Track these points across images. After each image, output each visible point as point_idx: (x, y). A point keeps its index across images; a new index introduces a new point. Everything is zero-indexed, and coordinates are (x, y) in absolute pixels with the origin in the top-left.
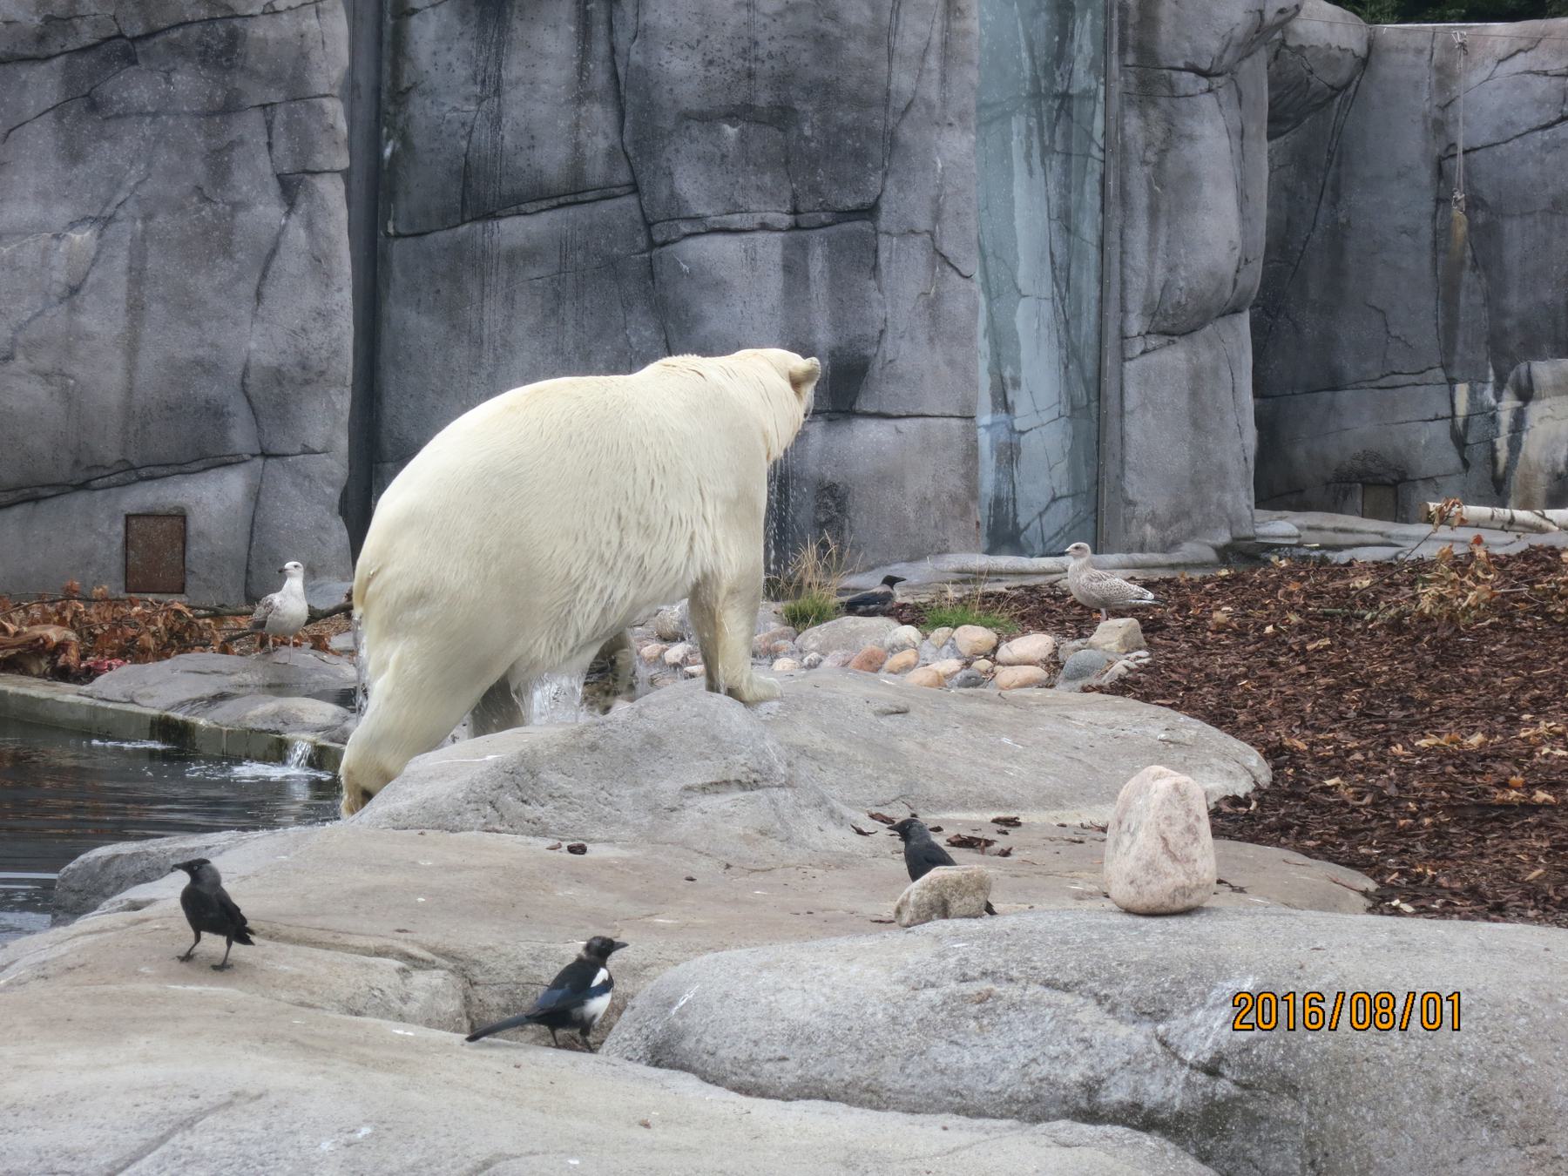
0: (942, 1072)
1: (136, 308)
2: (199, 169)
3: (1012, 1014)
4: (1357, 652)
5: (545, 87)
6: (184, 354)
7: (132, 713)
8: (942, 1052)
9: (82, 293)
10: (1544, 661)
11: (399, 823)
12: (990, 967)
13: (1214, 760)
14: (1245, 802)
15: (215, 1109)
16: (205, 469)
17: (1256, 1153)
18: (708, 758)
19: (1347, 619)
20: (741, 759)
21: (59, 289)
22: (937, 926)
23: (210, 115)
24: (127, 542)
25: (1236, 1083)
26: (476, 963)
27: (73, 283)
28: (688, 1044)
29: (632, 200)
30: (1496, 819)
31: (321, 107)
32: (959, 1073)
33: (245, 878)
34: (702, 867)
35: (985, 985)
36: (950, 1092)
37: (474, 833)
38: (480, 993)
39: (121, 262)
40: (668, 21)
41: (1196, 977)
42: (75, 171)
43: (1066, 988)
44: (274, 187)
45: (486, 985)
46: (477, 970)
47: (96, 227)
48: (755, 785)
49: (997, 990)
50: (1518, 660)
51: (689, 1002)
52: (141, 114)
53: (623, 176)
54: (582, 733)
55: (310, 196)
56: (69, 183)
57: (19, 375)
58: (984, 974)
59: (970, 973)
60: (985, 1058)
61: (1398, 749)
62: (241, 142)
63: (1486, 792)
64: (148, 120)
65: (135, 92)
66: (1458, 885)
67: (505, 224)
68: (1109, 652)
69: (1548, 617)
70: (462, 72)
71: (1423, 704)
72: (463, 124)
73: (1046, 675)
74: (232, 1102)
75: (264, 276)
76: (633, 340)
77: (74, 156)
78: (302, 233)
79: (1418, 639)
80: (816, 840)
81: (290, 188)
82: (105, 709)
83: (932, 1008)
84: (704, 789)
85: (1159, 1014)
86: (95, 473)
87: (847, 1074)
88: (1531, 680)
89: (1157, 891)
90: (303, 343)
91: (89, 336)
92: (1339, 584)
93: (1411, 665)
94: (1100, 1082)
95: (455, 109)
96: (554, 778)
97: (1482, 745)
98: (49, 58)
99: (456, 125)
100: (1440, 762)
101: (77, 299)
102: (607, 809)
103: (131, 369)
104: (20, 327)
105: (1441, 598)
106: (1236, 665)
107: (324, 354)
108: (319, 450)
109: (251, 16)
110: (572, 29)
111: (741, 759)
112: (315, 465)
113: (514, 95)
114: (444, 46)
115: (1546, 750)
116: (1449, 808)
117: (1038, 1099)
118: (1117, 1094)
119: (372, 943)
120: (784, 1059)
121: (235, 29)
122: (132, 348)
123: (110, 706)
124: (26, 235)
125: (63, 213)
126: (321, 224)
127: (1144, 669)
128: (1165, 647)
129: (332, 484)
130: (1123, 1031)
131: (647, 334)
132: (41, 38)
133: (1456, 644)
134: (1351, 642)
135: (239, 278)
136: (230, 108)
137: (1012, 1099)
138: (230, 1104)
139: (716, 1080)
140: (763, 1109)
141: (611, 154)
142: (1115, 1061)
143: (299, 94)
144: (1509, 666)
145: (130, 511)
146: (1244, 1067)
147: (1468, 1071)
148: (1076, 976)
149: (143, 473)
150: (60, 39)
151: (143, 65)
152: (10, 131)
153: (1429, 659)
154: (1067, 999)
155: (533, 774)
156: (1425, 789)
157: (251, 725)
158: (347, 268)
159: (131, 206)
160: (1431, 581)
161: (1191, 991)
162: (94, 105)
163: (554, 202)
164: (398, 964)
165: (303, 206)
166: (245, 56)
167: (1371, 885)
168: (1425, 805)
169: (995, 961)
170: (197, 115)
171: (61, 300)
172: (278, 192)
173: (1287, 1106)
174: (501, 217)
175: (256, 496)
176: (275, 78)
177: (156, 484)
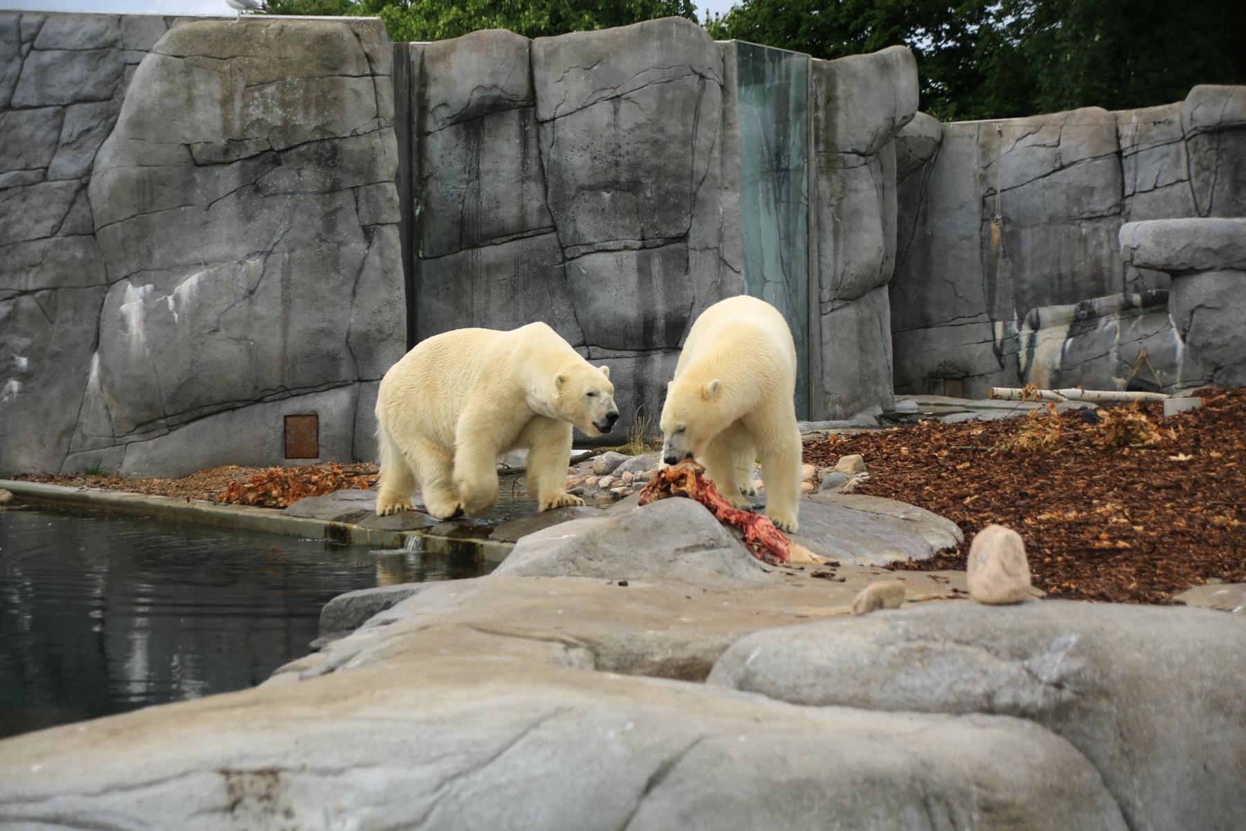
0: (904, 690)
1: (287, 302)
2: (319, 223)
3: (940, 658)
4: (988, 469)
5: (504, 174)
8: (902, 679)
9: (256, 293)
10: (1098, 471)
11: (523, 573)
12: (922, 633)
13: (933, 529)
14: (952, 551)
16: (328, 389)
17: (1087, 729)
18: (687, 533)
19: (974, 451)
20: (704, 533)
21: (243, 292)
22: (879, 614)
23: (323, 193)
25: (1075, 692)
26: (600, 644)
27: (252, 288)
28: (759, 679)
29: (553, 235)
30: (1099, 557)
31: (385, 188)
32: (914, 690)
33: (460, 604)
34: (692, 591)
35: (921, 643)
36: (908, 700)
37: (564, 577)
38: (603, 660)
39: (277, 276)
40: (571, 135)
41: (1042, 635)
42: (249, 226)
43: (968, 643)
44: (360, 232)
47: (263, 257)
48: (712, 547)
49: (930, 645)
50: (1083, 471)
51: (757, 658)
53: (547, 222)
54: (619, 522)
55: (380, 237)
56: (246, 232)
57: (221, 340)
58: (920, 637)
59: (913, 636)
60: (927, 682)
61: (1028, 521)
62: (341, 208)
63: (1087, 542)
64: (289, 196)
65: (281, 181)
66: (1092, 592)
67: (484, 250)
68: (847, 473)
69: (1093, 447)
70: (458, 167)
71: (1034, 496)
72: (460, 196)
73: (812, 487)
74: (557, 712)
75: (357, 282)
76: (556, 312)
77: (248, 218)
78: (377, 258)
79: (1022, 461)
80: (746, 575)
81: (369, 233)
82: (296, 523)
83: (894, 655)
84: (686, 550)
85: (1024, 656)
86: (266, 394)
87: (851, 692)
88: (1093, 481)
89: (1000, 592)
90: (380, 319)
91: (262, 318)
92: (964, 433)
93: (1021, 475)
94: (994, 693)
95: (455, 187)
96: (606, 546)
97: (1076, 518)
98: (231, 163)
99: (456, 196)
100: (1056, 527)
101: (253, 297)
102: (635, 562)
103: (285, 334)
104: (222, 314)
105: (1034, 438)
106: (919, 479)
107: (391, 324)
110: (518, 141)
111: (704, 533)
113: (486, 179)
114: (447, 152)
115: (1115, 519)
116: (1071, 552)
117: (959, 702)
118: (1004, 699)
119: (545, 635)
120: (814, 685)
121: (336, 145)
122: (285, 324)
123: (300, 520)
124: (223, 262)
125: (242, 250)
126: (387, 253)
127: (868, 482)
128: (876, 470)
130: (1004, 666)
131: (564, 308)
132: (226, 152)
133: (1045, 463)
134: (984, 464)
135: (343, 284)
136: (334, 189)
137: (945, 703)
139: (777, 697)
140: (811, 712)
141: (541, 210)
142: (1003, 680)
143: (371, 180)
144: (1077, 474)
146: (1077, 683)
147: (1208, 684)
148: (972, 637)
149: (294, 392)
150: (237, 152)
151: (285, 166)
153: (1030, 471)
154: (970, 650)
155: (594, 544)
156: (1053, 542)
157: (384, 527)
158: (402, 277)
159: (282, 245)
160: (1026, 429)
161: (1041, 643)
162: (258, 190)
163: (511, 238)
165: (376, 243)
166: (342, 161)
167: (1042, 593)
168: (1055, 550)
169: (925, 630)
170: (317, 193)
171: (244, 298)
172: (363, 235)
173: (1104, 704)
174: (481, 247)
175: (356, 403)
176: (358, 172)
177: (301, 398)
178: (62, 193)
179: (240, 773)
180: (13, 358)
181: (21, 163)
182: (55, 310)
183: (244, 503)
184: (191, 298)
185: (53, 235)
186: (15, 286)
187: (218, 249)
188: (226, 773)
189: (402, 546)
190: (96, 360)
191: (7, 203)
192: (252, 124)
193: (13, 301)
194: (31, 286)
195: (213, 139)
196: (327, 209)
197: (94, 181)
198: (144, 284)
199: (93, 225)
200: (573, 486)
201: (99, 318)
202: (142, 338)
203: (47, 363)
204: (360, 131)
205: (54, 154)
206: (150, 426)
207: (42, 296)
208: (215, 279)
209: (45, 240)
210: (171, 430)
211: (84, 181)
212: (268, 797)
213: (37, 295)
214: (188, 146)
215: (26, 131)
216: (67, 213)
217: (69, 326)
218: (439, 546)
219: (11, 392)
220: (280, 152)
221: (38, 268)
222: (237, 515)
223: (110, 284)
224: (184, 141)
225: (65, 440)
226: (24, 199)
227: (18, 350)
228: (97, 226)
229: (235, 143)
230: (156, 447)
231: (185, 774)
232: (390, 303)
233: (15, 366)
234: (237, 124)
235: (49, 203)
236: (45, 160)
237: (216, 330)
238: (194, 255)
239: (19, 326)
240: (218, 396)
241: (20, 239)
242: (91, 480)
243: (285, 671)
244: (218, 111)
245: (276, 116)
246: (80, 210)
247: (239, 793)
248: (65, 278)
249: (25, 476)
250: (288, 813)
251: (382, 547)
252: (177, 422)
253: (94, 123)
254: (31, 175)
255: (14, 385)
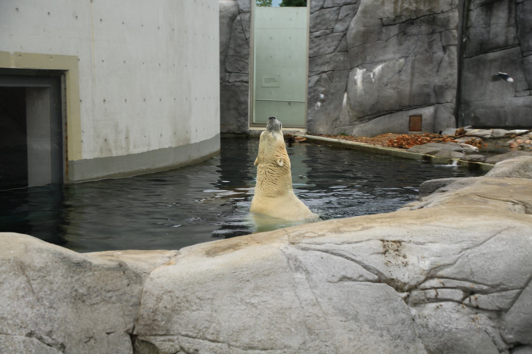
1: (413, 74)
2: (426, 45)
6: (422, 83)
7: (418, 155)
9: (402, 72)
11: (497, 176)
15: (505, 230)
21: (397, 71)
23: (429, 34)
24: (410, 121)
26: (528, 204)
29: (519, 48)
38: (529, 210)
39: (410, 65)
44: (442, 48)
45: (530, 208)
46: (527, 205)
52: (415, 35)
53: (517, 42)
56: (399, 50)
57: (389, 88)
62: (435, 40)
64: (416, 36)
65: (413, 31)
70: (482, 22)
74: (508, 228)
77: (400, 44)
81: (445, 49)
90: (447, 80)
91: (403, 80)
95: (480, 30)
98: (396, 24)
101: (401, 73)
103: (411, 86)
107: (451, 82)
108: (449, 101)
109: (438, 13)
112: (449, 105)
113: (493, 27)
119: (505, 199)
122: (412, 82)
125: (398, 56)
129: (452, 109)
132: (394, 20)
135: (434, 68)
136: (433, 33)
138: (508, 229)
141: (515, 38)
145: (411, 115)
149: (413, 107)
151: (415, 25)
152: (388, 39)
155: (527, 166)
164: (512, 203)
165: (447, 52)
170: (426, 34)
171: (398, 73)
175: (436, 112)
177: (416, 110)
178: (337, 37)
179: (388, 241)
180: (319, 95)
181: (325, 27)
182: (333, 78)
183: (393, 146)
184: (379, 73)
185: (334, 52)
186: (320, 70)
187: (389, 56)
188: (383, 241)
189: (451, 164)
190: (346, 95)
191: (320, 41)
192: (404, 10)
193: (320, 75)
194: (326, 70)
195: (390, 16)
196: (430, 40)
197: (348, 32)
198: (363, 69)
199: (347, 48)
200: (520, 144)
201: (347, 81)
202: (362, 88)
203: (330, 96)
204: (444, 11)
205: (336, 23)
206: (363, 119)
207: (329, 73)
208: (387, 67)
209: (331, 54)
210: (370, 120)
211: (345, 33)
212: (397, 250)
213: (328, 73)
214: (381, 19)
215: (328, 16)
216: (339, 44)
217: (337, 84)
218: (465, 165)
219: (318, 106)
220: (414, 20)
221: (328, 64)
222: (391, 151)
223: (352, 69)
224: (380, 17)
225: (335, 123)
226: (325, 40)
227: (321, 92)
228: (348, 49)
229: (398, 17)
230: (364, 126)
231: (368, 240)
232: (451, 75)
233: (319, 97)
234: (399, 10)
235: (333, 41)
236: (333, 26)
237: (387, 85)
238: (381, 58)
239: (322, 83)
240: (386, 108)
241: (323, 54)
242: (342, 137)
243: (406, 206)
244: (393, 6)
245: (413, 7)
246: (343, 43)
247: (388, 248)
248: (337, 67)
249: (321, 135)
250: (405, 257)
251: (444, 164)
252: (372, 117)
253: (349, 12)
254: (328, 31)
255: (319, 104)
